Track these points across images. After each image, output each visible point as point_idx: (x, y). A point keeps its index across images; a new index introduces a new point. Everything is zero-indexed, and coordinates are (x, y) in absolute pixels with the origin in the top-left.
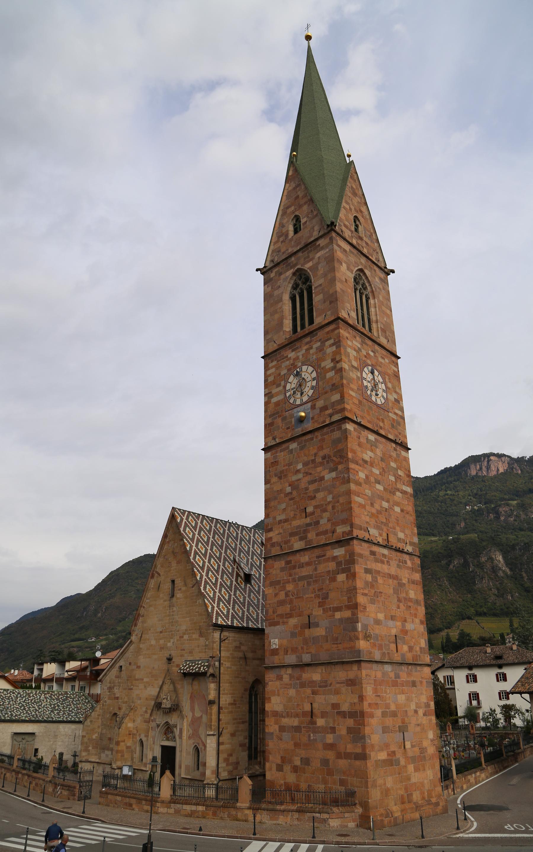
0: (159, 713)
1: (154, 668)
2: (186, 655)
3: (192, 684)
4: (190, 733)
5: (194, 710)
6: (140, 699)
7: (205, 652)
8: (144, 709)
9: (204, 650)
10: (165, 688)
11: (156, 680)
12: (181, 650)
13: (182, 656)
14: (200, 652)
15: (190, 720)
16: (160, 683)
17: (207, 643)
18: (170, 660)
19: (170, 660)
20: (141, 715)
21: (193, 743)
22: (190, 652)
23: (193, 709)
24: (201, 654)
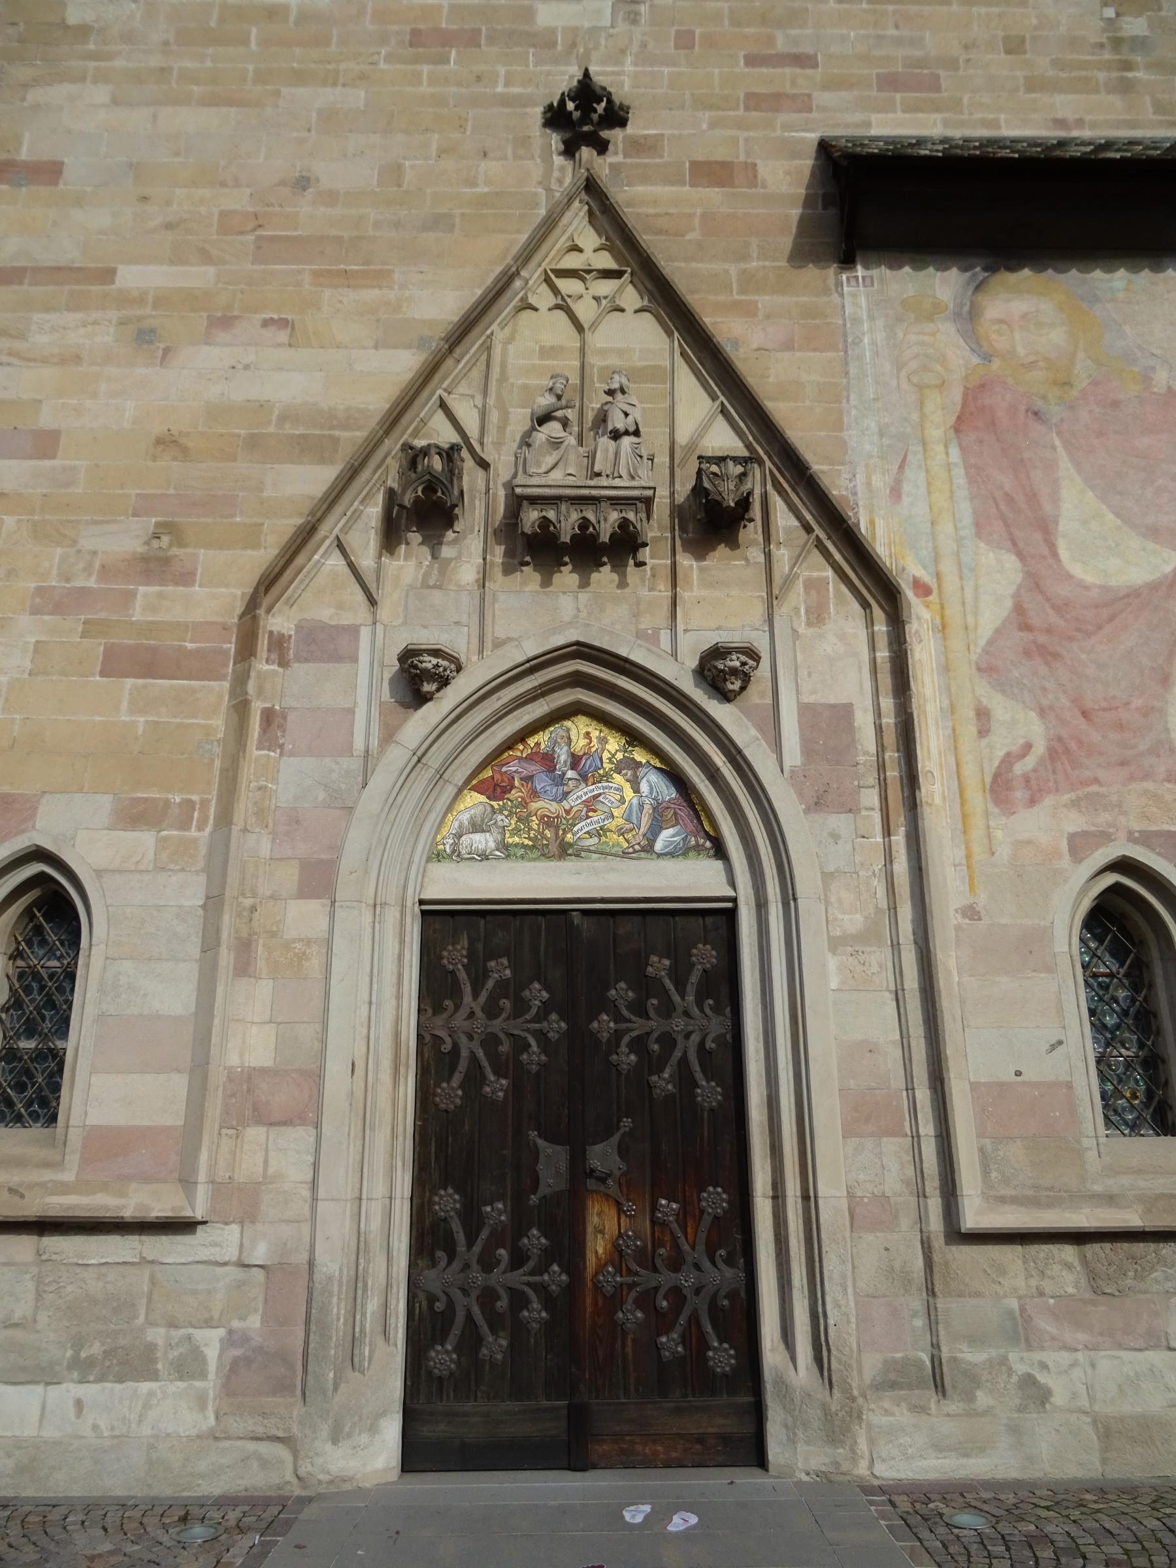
0: (409, 564)
1: (303, 183)
2: (823, 98)
3: (968, 319)
4: (1001, 744)
5: (1046, 528)
6: (46, 444)
7: (1125, 87)
8: (126, 539)
9: (1101, 76)
10: (531, 347)
11: (346, 279)
12: (751, 61)
13: (772, 102)
14: (1033, 84)
15: (990, 616)
16: (444, 304)
17: (1135, 26)
18: (585, 117)
19: (585, 117)
20: (51, 602)
21: (1078, 845)
22: (890, 82)
23: (1020, 521)
24: (1059, 99)
